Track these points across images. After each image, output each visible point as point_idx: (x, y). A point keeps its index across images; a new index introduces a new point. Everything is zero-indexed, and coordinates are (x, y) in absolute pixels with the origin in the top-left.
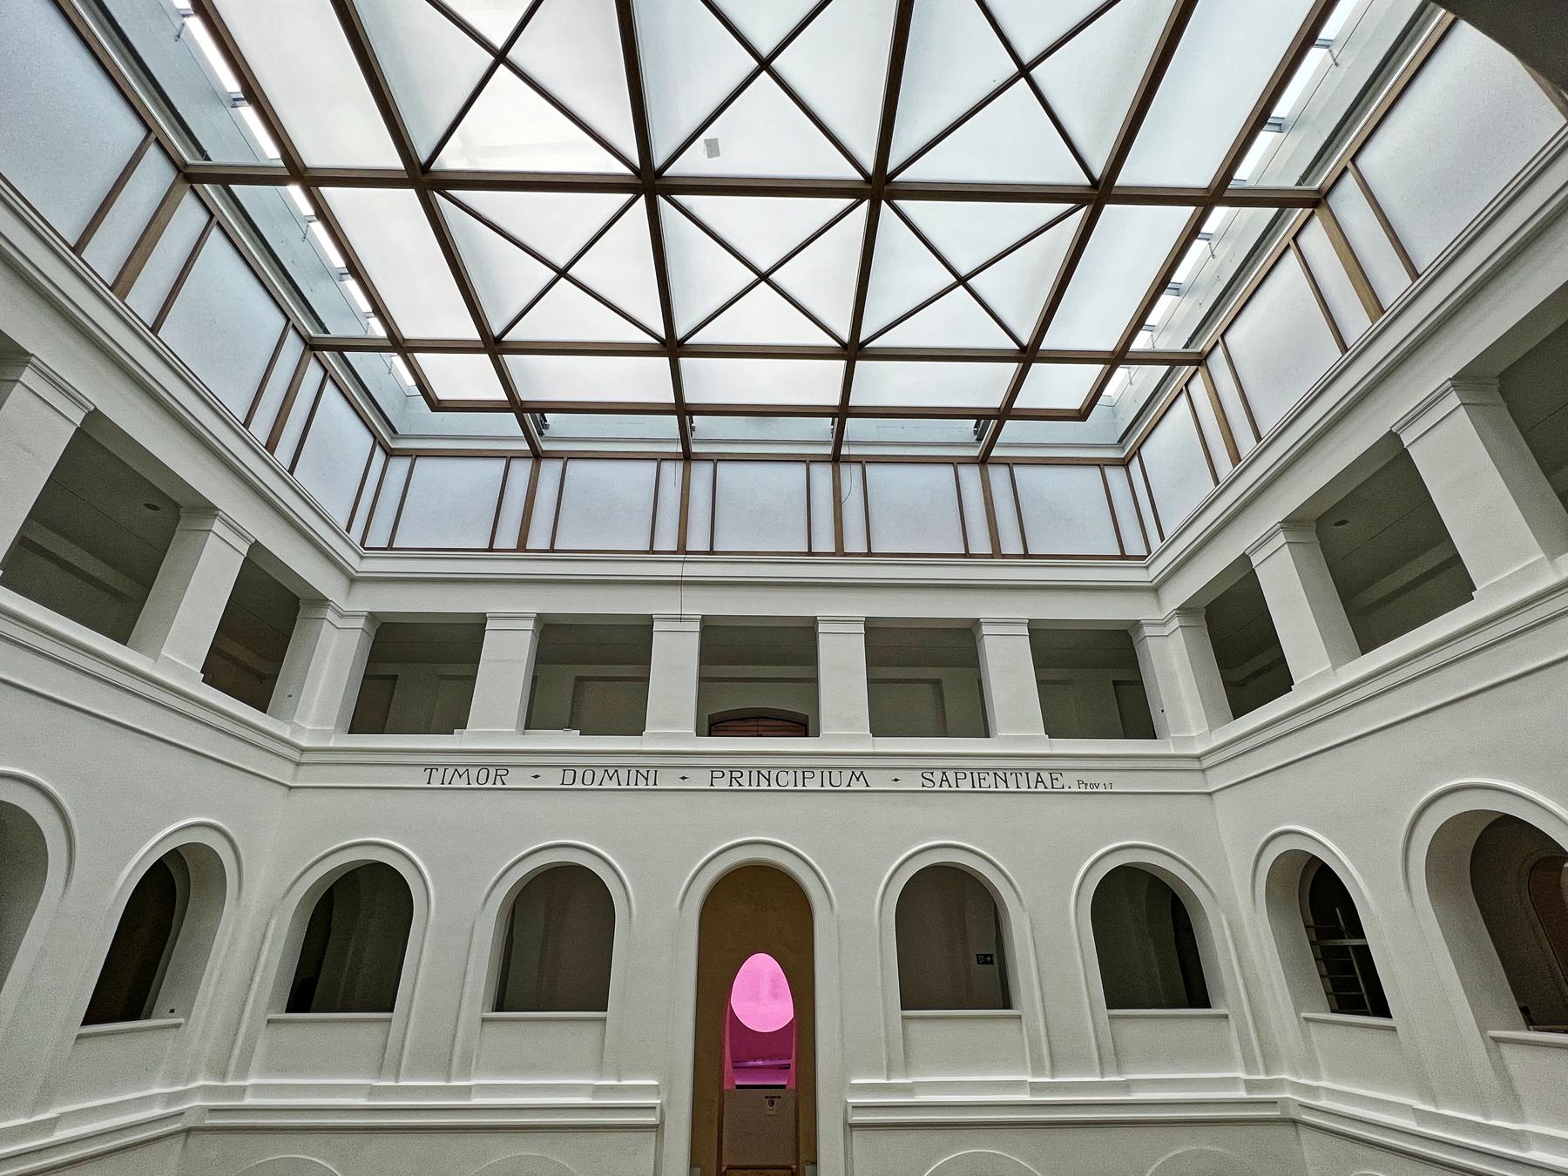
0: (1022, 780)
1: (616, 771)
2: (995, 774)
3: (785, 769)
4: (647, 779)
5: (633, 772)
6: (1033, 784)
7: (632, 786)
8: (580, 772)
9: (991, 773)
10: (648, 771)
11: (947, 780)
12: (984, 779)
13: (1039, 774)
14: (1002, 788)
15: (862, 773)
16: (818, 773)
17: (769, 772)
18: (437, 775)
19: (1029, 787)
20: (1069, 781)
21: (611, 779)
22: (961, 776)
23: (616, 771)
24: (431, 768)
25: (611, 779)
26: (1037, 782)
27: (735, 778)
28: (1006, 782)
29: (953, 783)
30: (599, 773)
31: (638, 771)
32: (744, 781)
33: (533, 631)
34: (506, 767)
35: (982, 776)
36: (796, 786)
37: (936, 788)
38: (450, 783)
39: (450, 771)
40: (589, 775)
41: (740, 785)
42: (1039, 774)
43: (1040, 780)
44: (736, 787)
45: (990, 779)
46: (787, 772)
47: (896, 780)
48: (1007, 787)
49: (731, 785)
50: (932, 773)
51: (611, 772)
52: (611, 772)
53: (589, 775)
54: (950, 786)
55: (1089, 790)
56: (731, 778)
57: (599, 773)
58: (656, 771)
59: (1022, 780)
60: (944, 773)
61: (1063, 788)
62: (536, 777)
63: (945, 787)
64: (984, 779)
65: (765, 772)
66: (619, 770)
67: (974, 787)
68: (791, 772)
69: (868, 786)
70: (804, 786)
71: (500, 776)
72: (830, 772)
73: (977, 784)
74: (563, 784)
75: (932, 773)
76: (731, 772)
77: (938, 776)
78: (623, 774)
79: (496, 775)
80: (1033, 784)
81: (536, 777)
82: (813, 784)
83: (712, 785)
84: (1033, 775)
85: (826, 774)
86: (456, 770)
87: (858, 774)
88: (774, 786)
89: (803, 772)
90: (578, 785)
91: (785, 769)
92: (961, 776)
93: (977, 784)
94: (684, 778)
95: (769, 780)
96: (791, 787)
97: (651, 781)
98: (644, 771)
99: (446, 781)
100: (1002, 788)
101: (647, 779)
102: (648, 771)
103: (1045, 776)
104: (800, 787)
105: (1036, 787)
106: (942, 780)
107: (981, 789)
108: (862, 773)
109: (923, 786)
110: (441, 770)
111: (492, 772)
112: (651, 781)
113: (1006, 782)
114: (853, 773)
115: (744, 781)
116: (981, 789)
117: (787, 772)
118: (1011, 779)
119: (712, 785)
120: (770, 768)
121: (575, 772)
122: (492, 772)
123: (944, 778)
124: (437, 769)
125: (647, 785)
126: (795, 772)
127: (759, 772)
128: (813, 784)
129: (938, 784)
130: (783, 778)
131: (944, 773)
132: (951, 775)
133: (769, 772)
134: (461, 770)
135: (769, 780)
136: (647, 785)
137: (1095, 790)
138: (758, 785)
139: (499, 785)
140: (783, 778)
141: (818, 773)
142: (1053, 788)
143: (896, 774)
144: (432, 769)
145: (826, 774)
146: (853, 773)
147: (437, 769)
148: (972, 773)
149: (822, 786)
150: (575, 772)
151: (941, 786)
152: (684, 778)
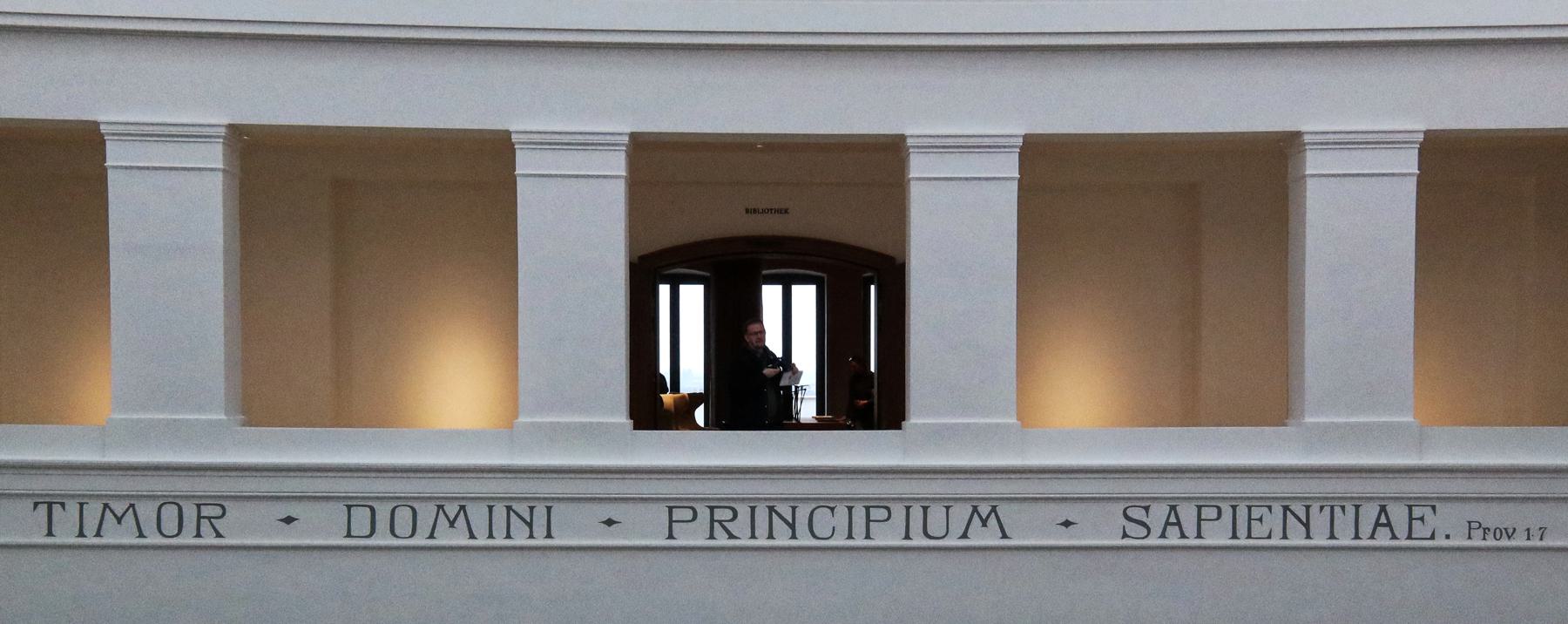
0: (1344, 522)
1: (463, 508)
2: (1286, 508)
3: (830, 505)
4: (530, 525)
5: (500, 512)
6: (1366, 529)
7: (500, 541)
8: (383, 512)
9: (1278, 508)
10: (532, 509)
11: (1178, 523)
12: (1260, 520)
13: (1383, 509)
14: (1297, 539)
15: (994, 509)
16: (898, 512)
17: (794, 509)
18: (66, 520)
19: (1357, 537)
20: (1449, 524)
21: (452, 524)
22: (1209, 513)
23: (463, 508)
24: (50, 504)
25: (452, 524)
26: (1377, 524)
27: (720, 522)
28: (1307, 525)
29: (1190, 529)
30: (427, 513)
31: (509, 508)
32: (741, 526)
33: (224, 171)
34: (220, 502)
35: (1256, 514)
36: (850, 537)
37: (1153, 541)
38: (98, 534)
39: (93, 511)
40: (404, 515)
41: (731, 536)
42: (1383, 509)
43: (1383, 520)
44: (722, 540)
45: (1274, 520)
46: (832, 509)
47: (1067, 524)
48: (1308, 537)
49: (712, 537)
50: (1147, 509)
51: (452, 510)
52: (452, 510)
53: (404, 515)
54: (1183, 536)
55: (1491, 542)
56: (712, 521)
57: (427, 513)
58: (549, 509)
59: (1344, 522)
60: (1173, 508)
61: (1432, 537)
62: (289, 520)
63: (1173, 539)
64: (1260, 520)
65: (785, 510)
66: (471, 509)
67: (1234, 536)
68: (842, 511)
69: (1005, 536)
70: (868, 537)
71: (209, 518)
72: (925, 509)
73: (1242, 531)
74: (349, 535)
75: (1147, 509)
76: (712, 509)
77: (1159, 513)
78: (478, 514)
79: (199, 517)
80: (1366, 529)
81: (289, 520)
82: (889, 536)
83: (671, 536)
84: (1370, 513)
85: (917, 513)
86: (106, 506)
87: (986, 513)
88: (805, 540)
89: (868, 509)
90: (382, 539)
91: (830, 505)
92: (1209, 513)
93: (1242, 531)
94: (610, 522)
95: (792, 526)
96: (840, 541)
97: (539, 529)
98: (522, 508)
99: (91, 528)
100: (1297, 539)
101: (530, 525)
102: (532, 509)
103: (1398, 514)
104: (859, 541)
105: (1372, 537)
106: (1167, 523)
107: (1251, 542)
108: (994, 509)
109: (1125, 535)
110: (72, 507)
111: (190, 513)
112: (539, 529)
113: (1307, 525)
114: (975, 509)
115: (741, 526)
116: (1251, 542)
117: (832, 509)
118: (1319, 521)
119: (671, 536)
120: (794, 503)
121: (372, 510)
122: (190, 513)
123: (1173, 519)
124: (63, 505)
125: (531, 536)
126: (850, 509)
127: (771, 509)
128: (889, 536)
129: (1157, 529)
130: (823, 520)
131: (1173, 508)
132: (1188, 514)
133: (794, 509)
134: (119, 507)
135: (792, 526)
136: (531, 536)
137: (1505, 542)
138: (771, 536)
139: (209, 539)
140: (823, 520)
141: (898, 512)
142: (1409, 537)
143: (1067, 512)
144: (50, 505)
145: (917, 513)
146: (975, 509)
147: (63, 505)
148: (1234, 508)
149: (907, 537)
150: (372, 510)
151: (1163, 536)
152: (610, 522)
